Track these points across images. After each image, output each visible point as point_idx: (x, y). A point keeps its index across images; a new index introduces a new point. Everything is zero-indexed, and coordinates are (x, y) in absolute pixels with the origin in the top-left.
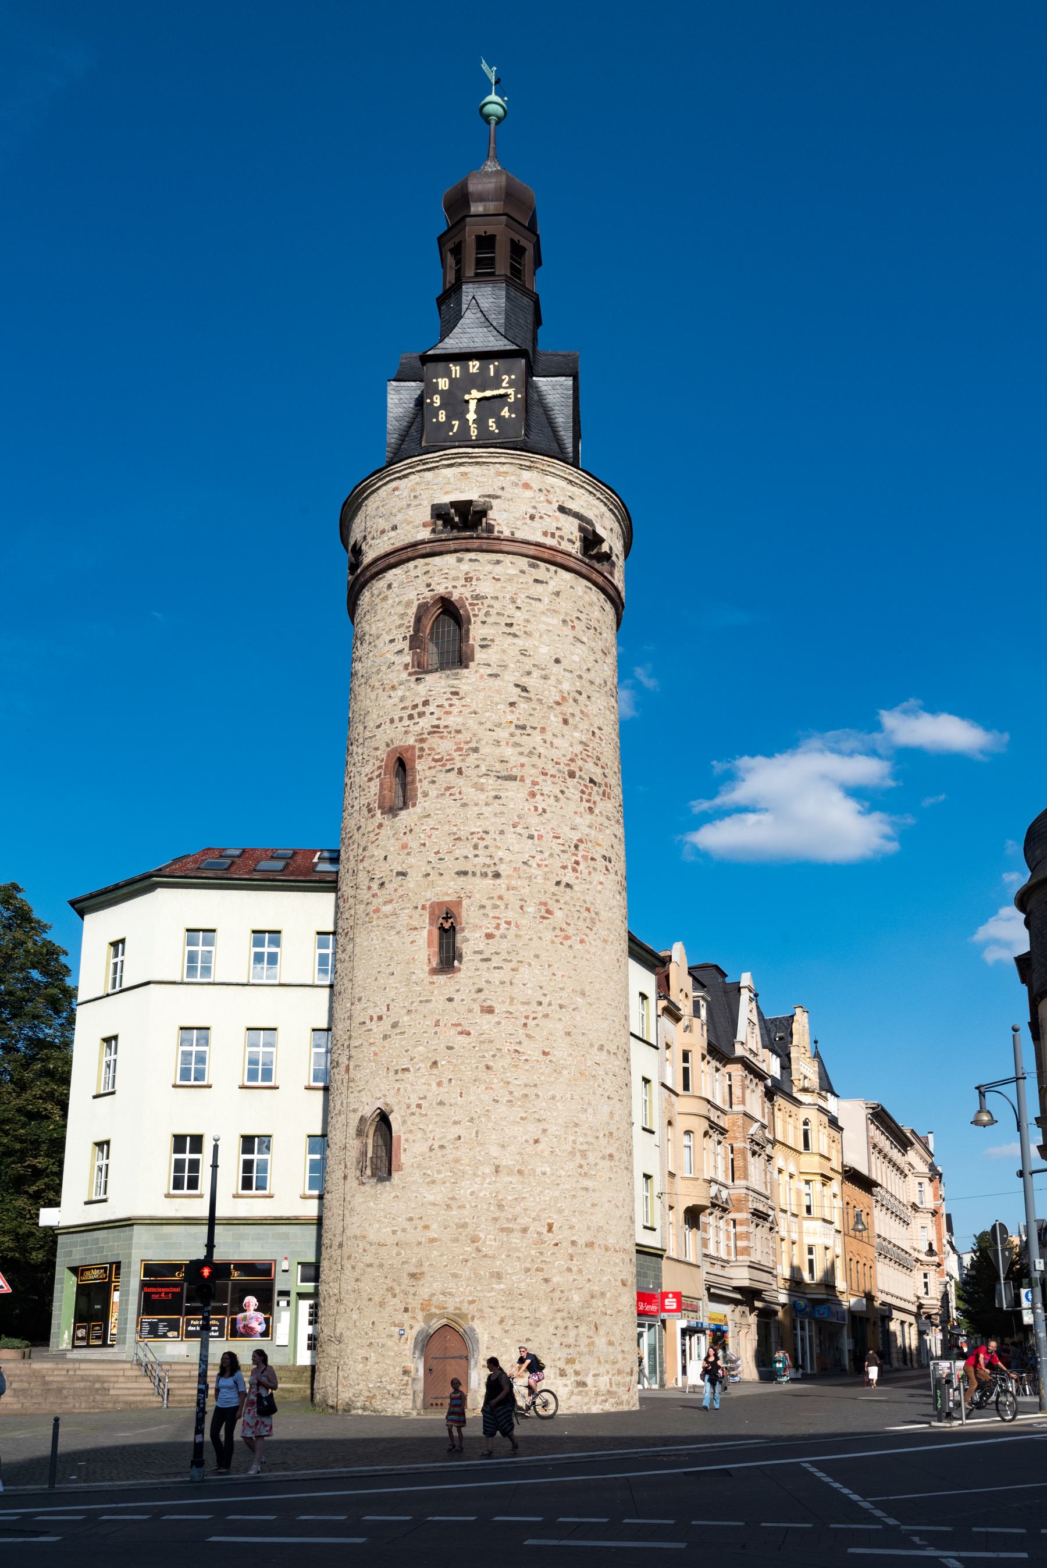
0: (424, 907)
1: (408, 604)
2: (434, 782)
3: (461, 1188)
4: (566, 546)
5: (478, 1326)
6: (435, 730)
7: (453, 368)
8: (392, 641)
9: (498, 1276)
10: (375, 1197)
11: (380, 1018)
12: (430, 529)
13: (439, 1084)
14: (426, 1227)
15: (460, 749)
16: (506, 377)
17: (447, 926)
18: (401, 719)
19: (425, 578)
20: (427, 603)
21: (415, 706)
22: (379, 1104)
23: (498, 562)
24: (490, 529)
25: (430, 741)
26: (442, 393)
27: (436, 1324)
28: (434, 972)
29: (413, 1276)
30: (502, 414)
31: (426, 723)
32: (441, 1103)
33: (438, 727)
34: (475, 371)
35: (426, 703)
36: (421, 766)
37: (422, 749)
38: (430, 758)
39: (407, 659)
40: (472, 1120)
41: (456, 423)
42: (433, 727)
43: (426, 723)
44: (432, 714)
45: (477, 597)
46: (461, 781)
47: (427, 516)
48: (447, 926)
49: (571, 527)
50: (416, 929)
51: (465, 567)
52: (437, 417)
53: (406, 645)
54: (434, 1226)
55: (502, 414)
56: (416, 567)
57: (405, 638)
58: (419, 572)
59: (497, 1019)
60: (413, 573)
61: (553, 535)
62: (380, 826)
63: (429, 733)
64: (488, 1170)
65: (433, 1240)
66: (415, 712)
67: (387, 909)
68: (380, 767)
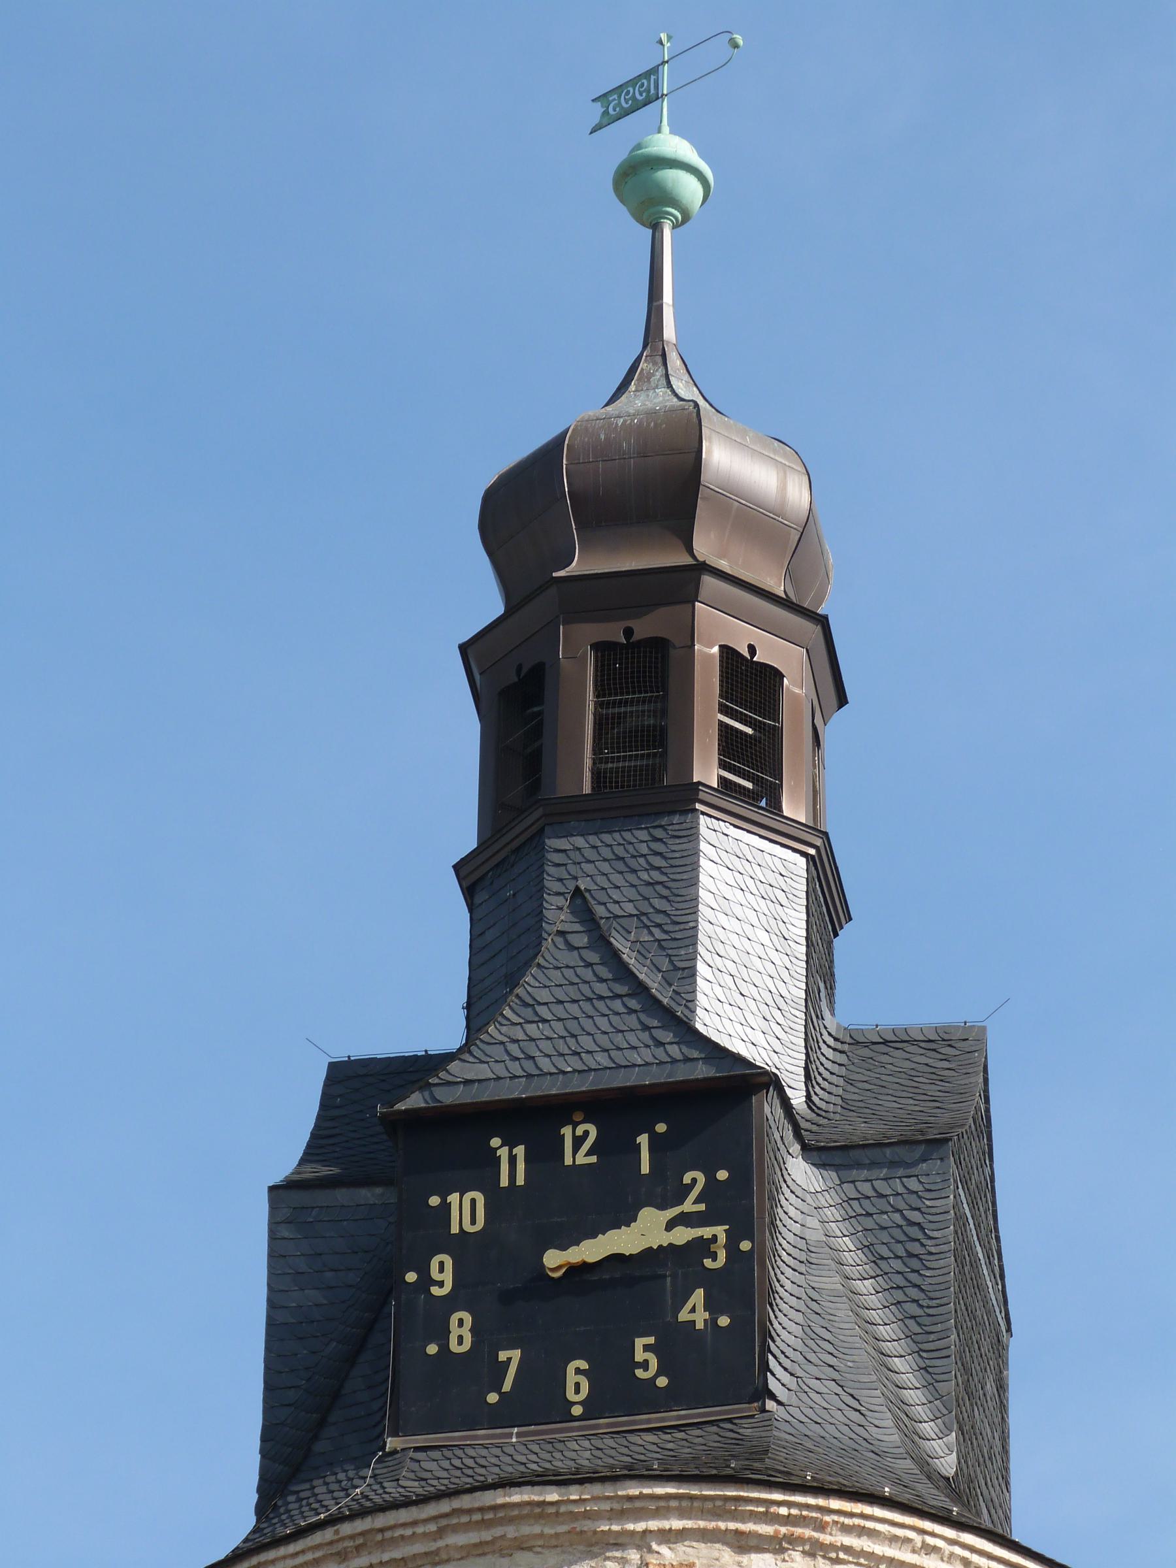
7: (503, 1153)
16: (696, 1177)
26: (460, 1246)
30: (684, 1316)
34: (582, 1159)
41: (512, 1356)
55: (684, 1316)
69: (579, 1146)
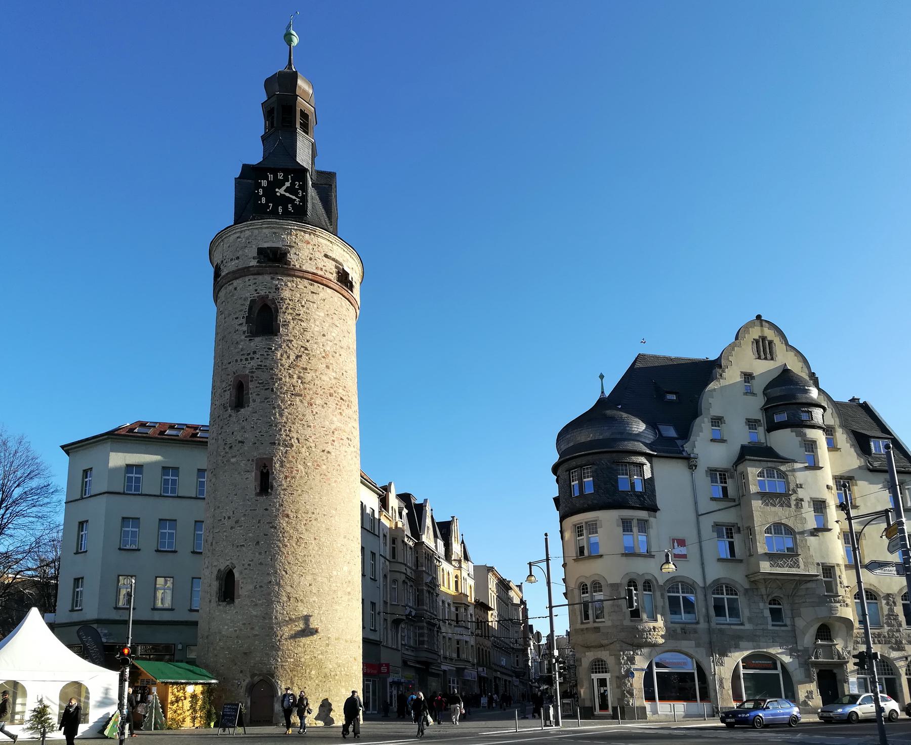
0: (253, 460)
1: (245, 299)
4: (328, 275)
6: (259, 367)
8: (237, 318)
10: (225, 612)
11: (229, 518)
13: (260, 554)
14: (252, 629)
17: (265, 471)
18: (241, 360)
21: (249, 354)
22: (228, 563)
24: (288, 263)
26: (263, 188)
27: (256, 679)
29: (245, 654)
31: (253, 363)
32: (261, 564)
35: (255, 353)
37: (252, 377)
39: (245, 328)
41: (271, 205)
43: (253, 363)
48: (265, 471)
49: (331, 266)
53: (244, 321)
54: (257, 628)
60: (248, 283)
61: (321, 269)
62: (230, 416)
65: (256, 635)
66: (249, 357)
67: (233, 460)
69: (280, 176)
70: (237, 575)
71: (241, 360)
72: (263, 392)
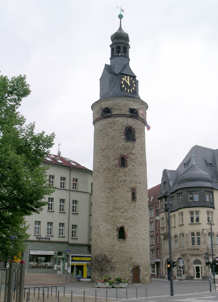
1: (124, 126)
2: (131, 164)
3: (138, 242)
5: (141, 268)
9: (143, 259)
11: (121, 208)
12: (129, 113)
15: (135, 158)
17: (133, 192)
18: (123, 149)
19: (127, 122)
20: (127, 127)
21: (126, 147)
23: (138, 122)
24: (138, 115)
25: (129, 155)
28: (132, 201)
29: (131, 258)
33: (131, 153)
36: (128, 160)
38: (130, 159)
40: (139, 230)
42: (130, 152)
44: (130, 150)
45: (136, 128)
46: (135, 164)
47: (128, 110)
48: (133, 192)
50: (128, 192)
51: (134, 121)
52: (123, 86)
53: (123, 134)
56: (125, 119)
57: (123, 133)
58: (125, 120)
59: (141, 211)
63: (129, 154)
64: (141, 239)
65: (134, 252)
66: (126, 148)
68: (118, 158)
70: (126, 230)
71: (123, 149)
72: (132, 163)
